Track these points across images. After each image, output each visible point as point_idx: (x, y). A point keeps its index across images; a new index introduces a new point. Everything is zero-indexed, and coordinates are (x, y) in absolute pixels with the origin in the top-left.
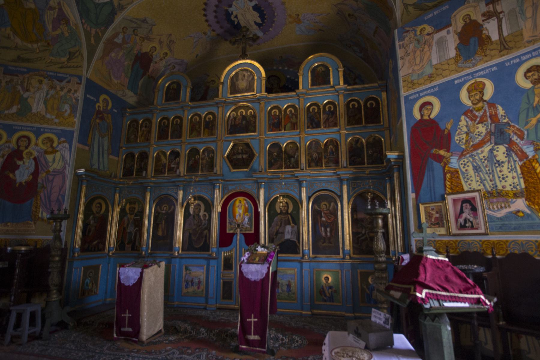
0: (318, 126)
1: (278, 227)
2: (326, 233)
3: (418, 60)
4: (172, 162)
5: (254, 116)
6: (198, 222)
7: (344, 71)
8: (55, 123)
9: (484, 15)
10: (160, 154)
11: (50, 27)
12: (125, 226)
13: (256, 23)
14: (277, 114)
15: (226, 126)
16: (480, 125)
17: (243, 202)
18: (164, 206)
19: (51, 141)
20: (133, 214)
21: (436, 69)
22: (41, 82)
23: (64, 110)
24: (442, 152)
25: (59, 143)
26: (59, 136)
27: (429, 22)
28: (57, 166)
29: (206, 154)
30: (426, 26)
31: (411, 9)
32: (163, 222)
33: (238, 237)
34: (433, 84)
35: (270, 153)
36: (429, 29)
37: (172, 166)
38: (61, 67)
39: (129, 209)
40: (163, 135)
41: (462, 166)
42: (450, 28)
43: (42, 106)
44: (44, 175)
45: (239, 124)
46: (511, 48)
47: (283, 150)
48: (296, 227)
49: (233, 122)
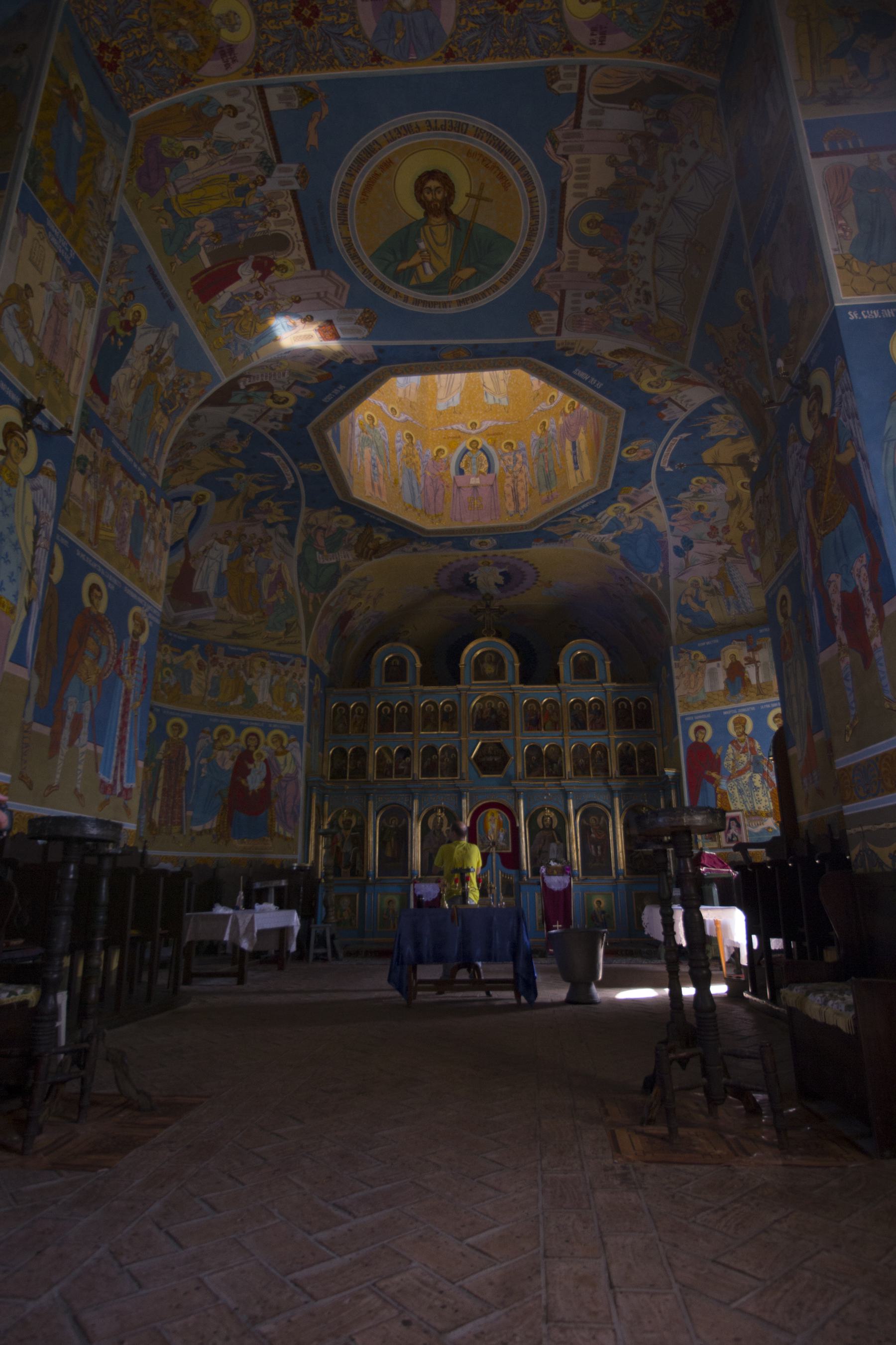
0: (584, 727)
2: (596, 850)
3: (692, 684)
5: (506, 710)
7: (611, 665)
8: (283, 717)
9: (746, 659)
11: (265, 593)
13: (496, 584)
14: (535, 709)
16: (743, 755)
17: (497, 815)
19: (279, 738)
21: (709, 697)
22: (263, 665)
23: (291, 701)
24: (714, 775)
25: (290, 742)
26: (288, 733)
27: (702, 649)
28: (288, 770)
29: (446, 754)
30: (698, 652)
31: (685, 627)
32: (393, 840)
33: (494, 857)
34: (705, 710)
35: (528, 756)
36: (702, 657)
38: (279, 644)
39: (343, 823)
40: (385, 724)
41: (729, 788)
42: (720, 662)
43: (267, 696)
44: (277, 781)
46: (765, 695)
48: (562, 845)
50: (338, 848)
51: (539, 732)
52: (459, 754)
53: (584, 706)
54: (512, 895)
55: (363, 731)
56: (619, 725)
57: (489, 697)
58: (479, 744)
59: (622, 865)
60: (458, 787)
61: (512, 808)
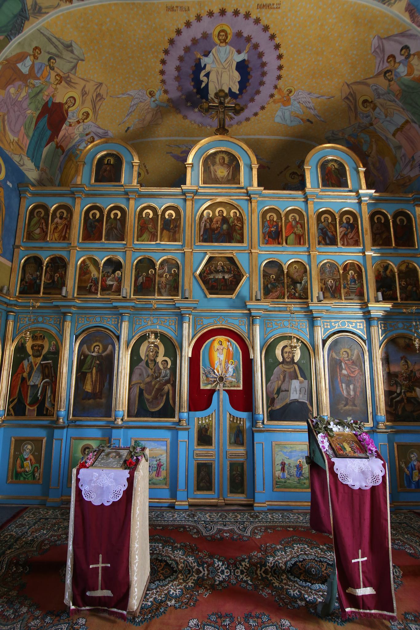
0: (333, 242)
1: (280, 382)
4: (108, 277)
5: (240, 219)
6: (155, 372)
7: (365, 173)
10: (88, 262)
12: (25, 375)
14: (275, 219)
15: (197, 228)
17: (225, 344)
18: (95, 344)
20: (40, 356)
29: (166, 268)
33: (221, 396)
35: (266, 275)
37: (109, 283)
39: (32, 348)
45: (217, 228)
47: (286, 271)
48: (306, 382)
49: (208, 225)
50: (23, 379)
51: (280, 246)
52: (181, 267)
53: (334, 218)
54: (242, 444)
55: (65, 238)
56: (375, 242)
57: (220, 204)
58: (207, 257)
59: (382, 413)
60: (179, 308)
61: (245, 335)
